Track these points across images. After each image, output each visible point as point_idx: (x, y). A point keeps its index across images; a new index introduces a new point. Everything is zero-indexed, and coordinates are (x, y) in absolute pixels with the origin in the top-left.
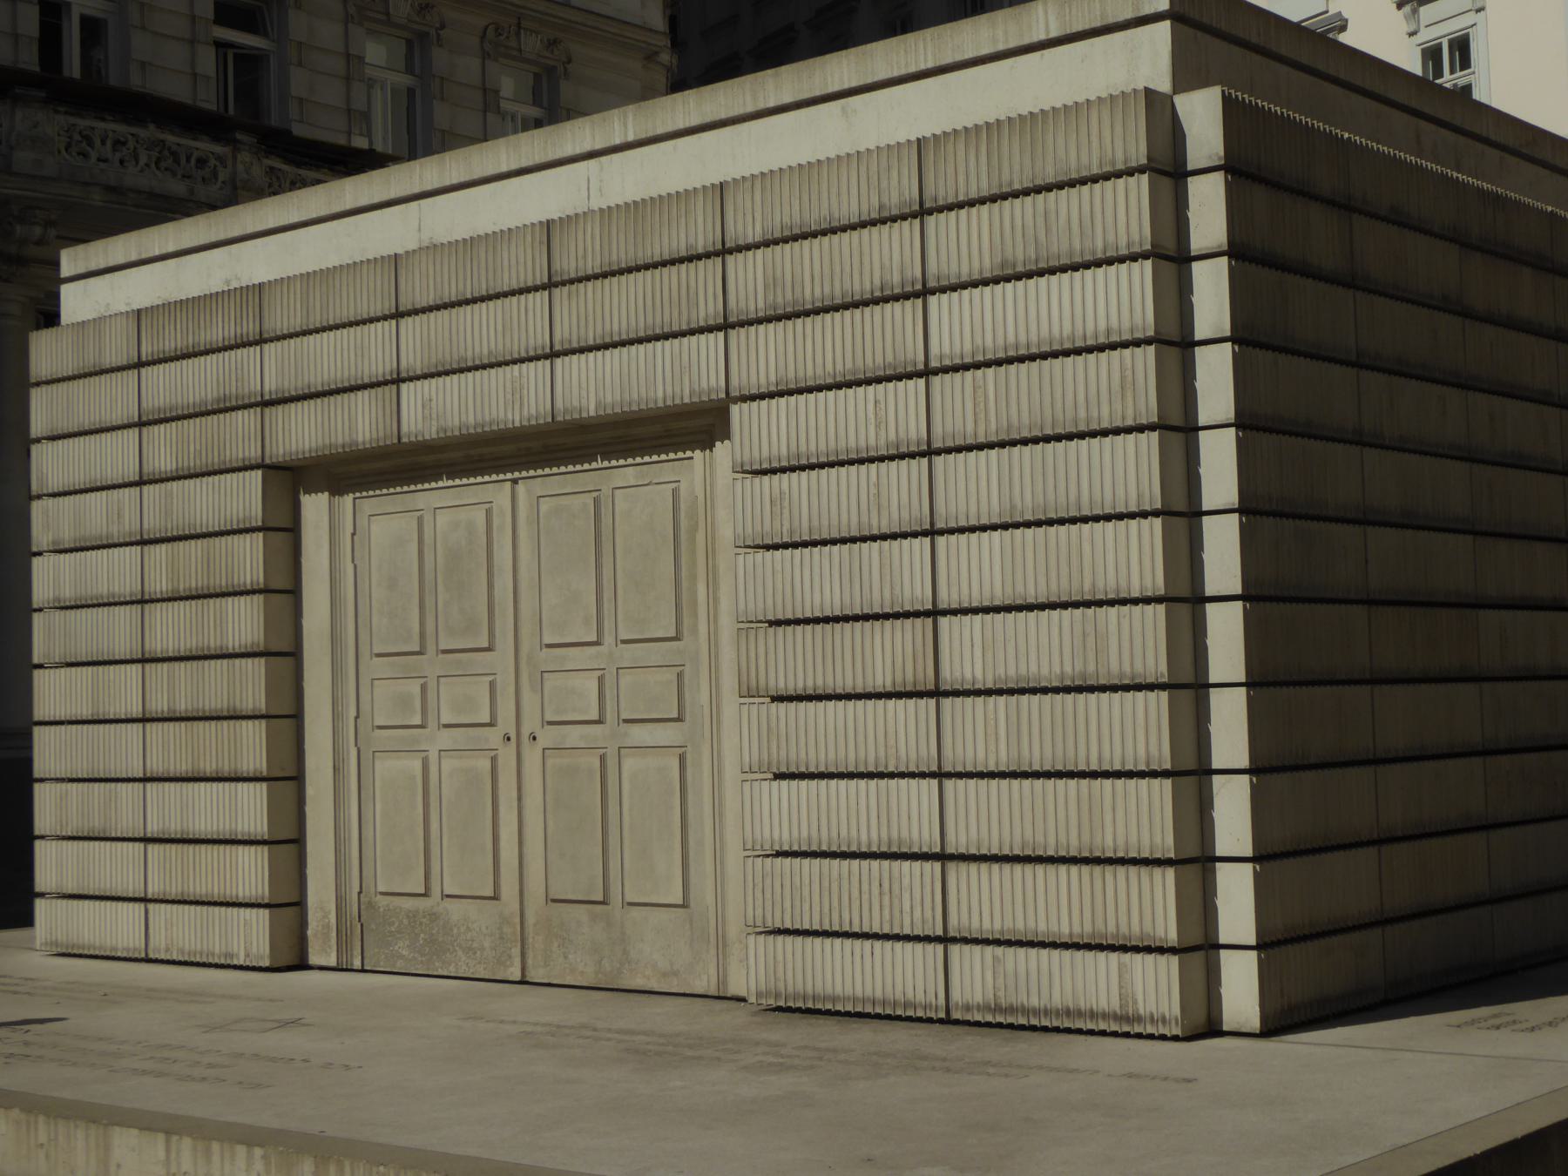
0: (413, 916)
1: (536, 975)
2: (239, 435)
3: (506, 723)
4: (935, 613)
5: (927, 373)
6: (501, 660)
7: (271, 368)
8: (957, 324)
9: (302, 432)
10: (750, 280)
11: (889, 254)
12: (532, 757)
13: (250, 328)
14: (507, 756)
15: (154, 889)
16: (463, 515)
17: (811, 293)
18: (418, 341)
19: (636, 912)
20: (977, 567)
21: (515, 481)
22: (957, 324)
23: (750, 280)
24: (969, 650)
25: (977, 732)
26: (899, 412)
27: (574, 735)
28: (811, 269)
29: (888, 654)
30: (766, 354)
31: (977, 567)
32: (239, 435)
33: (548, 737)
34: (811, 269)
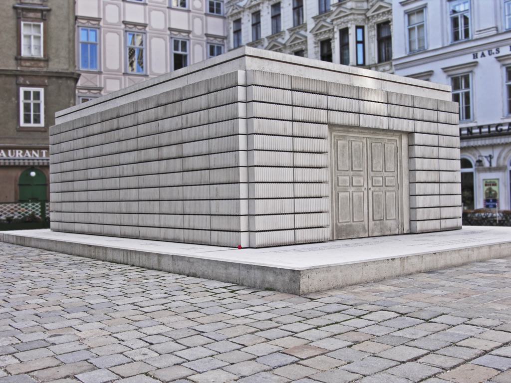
0: (347, 226)
1: (370, 236)
2: (322, 116)
3: (365, 186)
4: (439, 171)
5: (438, 134)
6: (364, 173)
7: (332, 102)
9: (337, 118)
10: (418, 113)
11: (432, 115)
12: (370, 192)
13: (324, 90)
14: (366, 192)
15: (297, 226)
16: (357, 143)
17: (425, 119)
19: (387, 221)
21: (367, 138)
23: (418, 113)
27: (377, 189)
29: (433, 176)
30: (420, 126)
33: (373, 189)
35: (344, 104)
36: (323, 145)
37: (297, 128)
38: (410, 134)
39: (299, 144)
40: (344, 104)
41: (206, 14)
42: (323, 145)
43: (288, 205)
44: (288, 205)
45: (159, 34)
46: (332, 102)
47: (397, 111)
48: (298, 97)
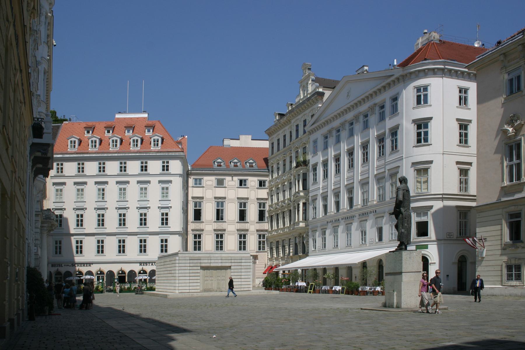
7: (202, 261)
8: (242, 264)
9: (203, 265)
10: (233, 261)
11: (239, 261)
18: (212, 261)
20: (243, 274)
22: (242, 264)
23: (233, 261)
24: (243, 277)
25: (242, 280)
26: (240, 267)
28: (236, 261)
30: (233, 264)
31: (243, 274)
32: (199, 265)
34: (236, 261)
35: (206, 261)
36: (199, 271)
37: (191, 268)
38: (230, 267)
39: (191, 271)
40: (206, 261)
41: (257, 188)
42: (199, 271)
43: (188, 285)
44: (188, 285)
45: (232, 201)
46: (202, 261)
47: (224, 261)
48: (191, 261)
